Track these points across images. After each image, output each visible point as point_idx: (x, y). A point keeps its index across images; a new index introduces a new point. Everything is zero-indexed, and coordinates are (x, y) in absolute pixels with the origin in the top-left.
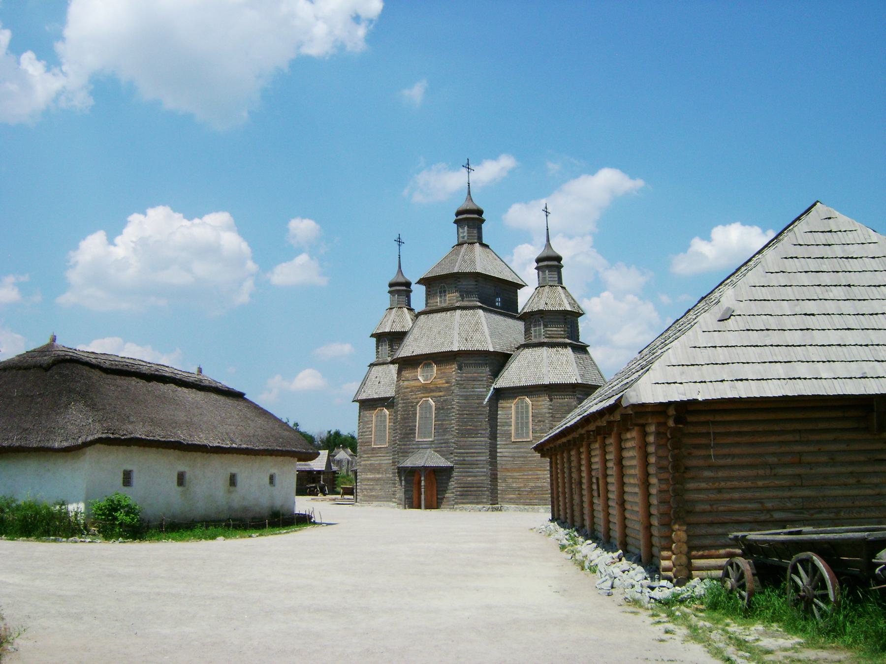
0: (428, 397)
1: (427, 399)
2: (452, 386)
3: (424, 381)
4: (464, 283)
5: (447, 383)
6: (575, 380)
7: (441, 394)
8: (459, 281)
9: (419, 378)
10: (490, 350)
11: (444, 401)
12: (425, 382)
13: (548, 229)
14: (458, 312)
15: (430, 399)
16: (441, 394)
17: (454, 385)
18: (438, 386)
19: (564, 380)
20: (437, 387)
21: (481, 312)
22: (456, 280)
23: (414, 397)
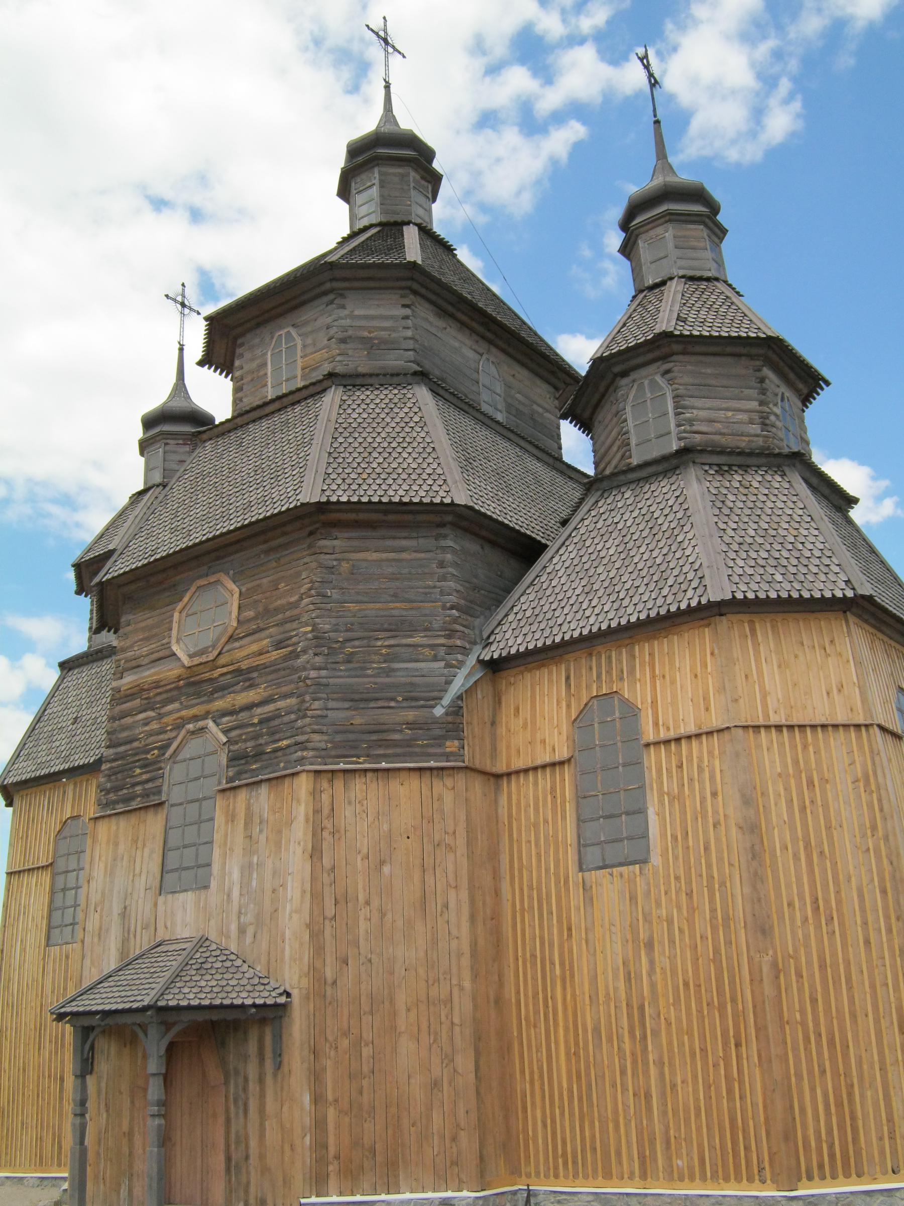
0: (205, 717)
1: (201, 724)
2: (298, 656)
3: (191, 656)
4: (357, 313)
5: (279, 645)
6: (843, 585)
7: (252, 696)
8: (343, 307)
9: (175, 648)
10: (456, 502)
11: (261, 722)
12: (197, 660)
13: (657, 122)
14: (333, 397)
15: (211, 724)
16: (252, 696)
17: (304, 651)
18: (244, 665)
19: (797, 586)
20: (239, 672)
21: (422, 394)
22: (332, 302)
23: (154, 726)
